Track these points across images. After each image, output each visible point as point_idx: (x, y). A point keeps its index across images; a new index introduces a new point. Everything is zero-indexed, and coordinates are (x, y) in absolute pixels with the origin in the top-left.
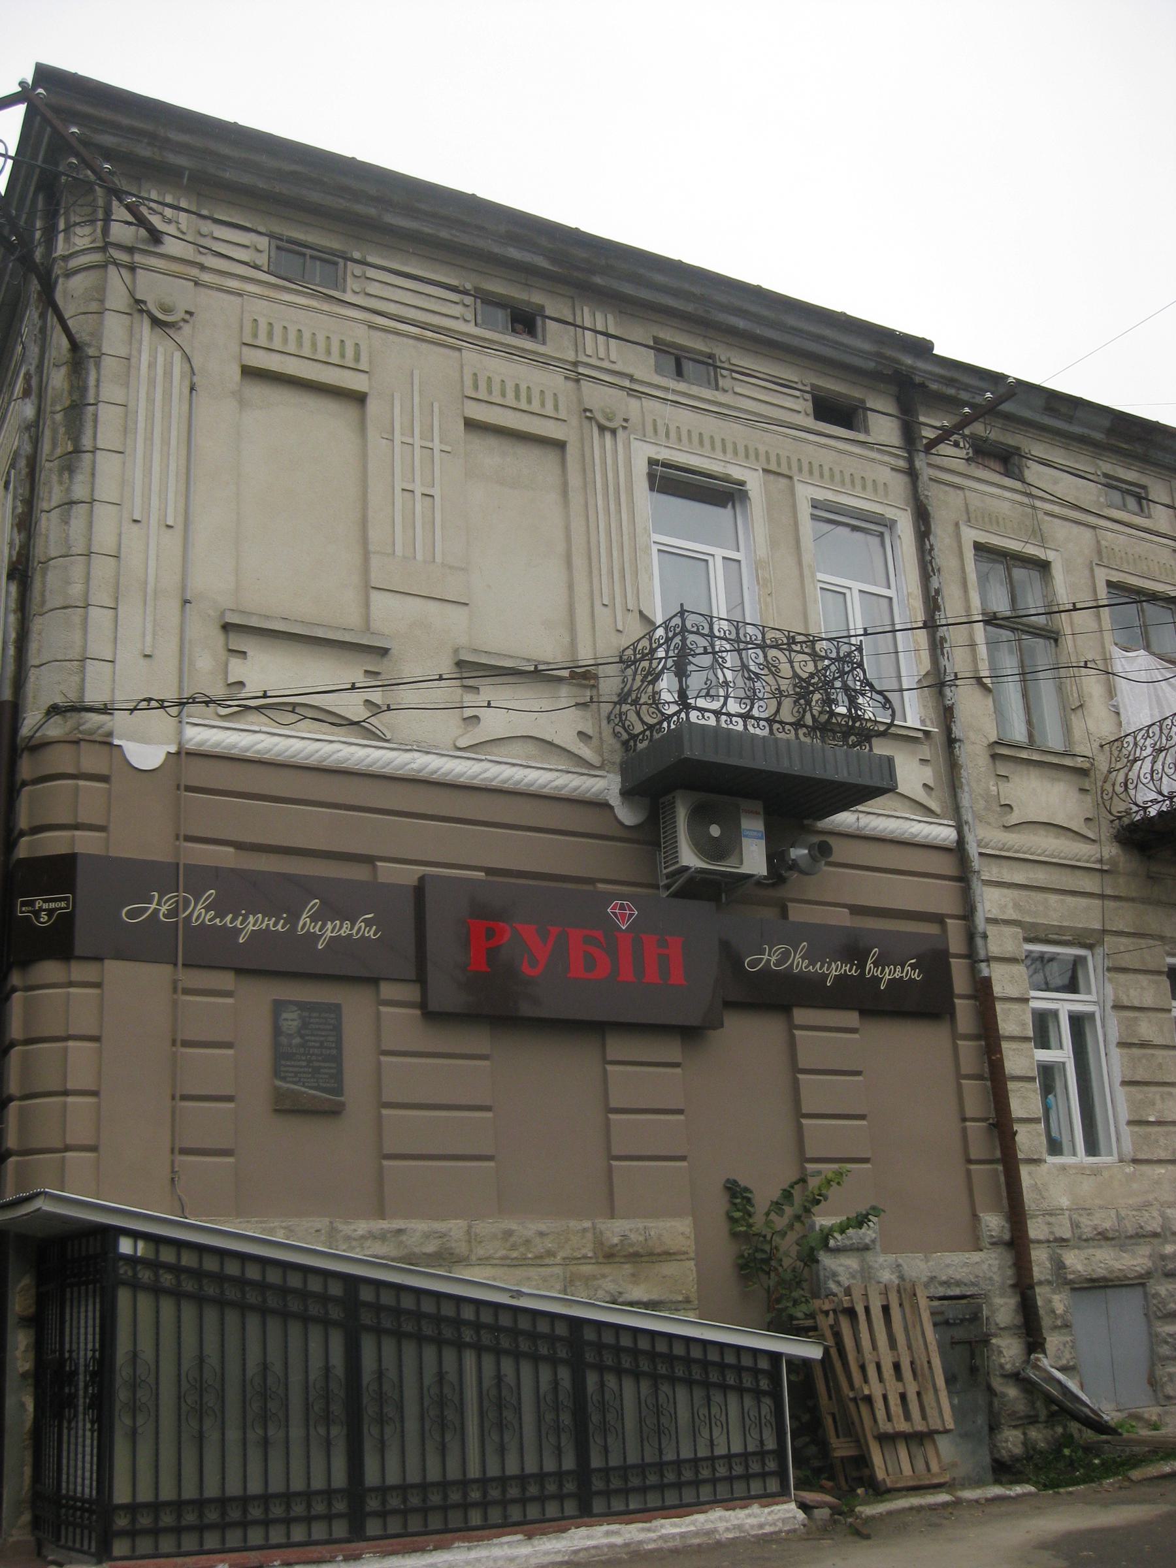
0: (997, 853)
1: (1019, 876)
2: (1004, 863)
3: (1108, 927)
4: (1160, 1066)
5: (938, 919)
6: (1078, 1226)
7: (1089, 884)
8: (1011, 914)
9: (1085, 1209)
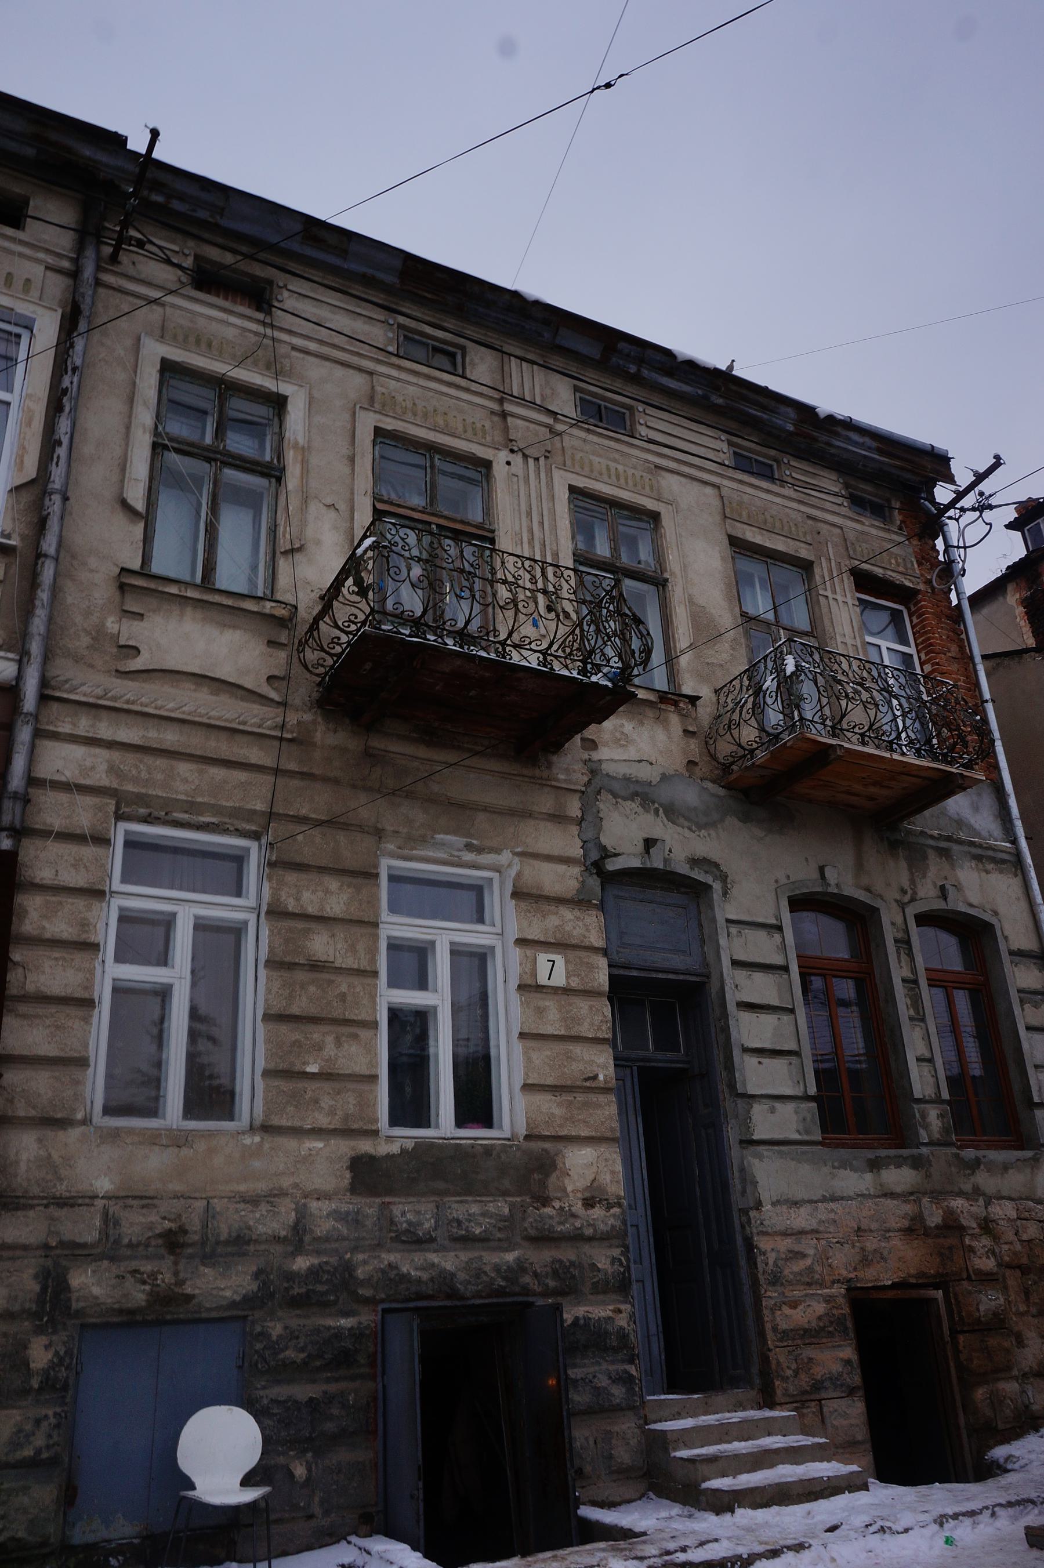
0: (91, 700)
1: (129, 733)
2: (104, 714)
3: (279, 809)
4: (343, 997)
6: (117, 1223)
7: (255, 754)
8: (101, 778)
9: (141, 1198)
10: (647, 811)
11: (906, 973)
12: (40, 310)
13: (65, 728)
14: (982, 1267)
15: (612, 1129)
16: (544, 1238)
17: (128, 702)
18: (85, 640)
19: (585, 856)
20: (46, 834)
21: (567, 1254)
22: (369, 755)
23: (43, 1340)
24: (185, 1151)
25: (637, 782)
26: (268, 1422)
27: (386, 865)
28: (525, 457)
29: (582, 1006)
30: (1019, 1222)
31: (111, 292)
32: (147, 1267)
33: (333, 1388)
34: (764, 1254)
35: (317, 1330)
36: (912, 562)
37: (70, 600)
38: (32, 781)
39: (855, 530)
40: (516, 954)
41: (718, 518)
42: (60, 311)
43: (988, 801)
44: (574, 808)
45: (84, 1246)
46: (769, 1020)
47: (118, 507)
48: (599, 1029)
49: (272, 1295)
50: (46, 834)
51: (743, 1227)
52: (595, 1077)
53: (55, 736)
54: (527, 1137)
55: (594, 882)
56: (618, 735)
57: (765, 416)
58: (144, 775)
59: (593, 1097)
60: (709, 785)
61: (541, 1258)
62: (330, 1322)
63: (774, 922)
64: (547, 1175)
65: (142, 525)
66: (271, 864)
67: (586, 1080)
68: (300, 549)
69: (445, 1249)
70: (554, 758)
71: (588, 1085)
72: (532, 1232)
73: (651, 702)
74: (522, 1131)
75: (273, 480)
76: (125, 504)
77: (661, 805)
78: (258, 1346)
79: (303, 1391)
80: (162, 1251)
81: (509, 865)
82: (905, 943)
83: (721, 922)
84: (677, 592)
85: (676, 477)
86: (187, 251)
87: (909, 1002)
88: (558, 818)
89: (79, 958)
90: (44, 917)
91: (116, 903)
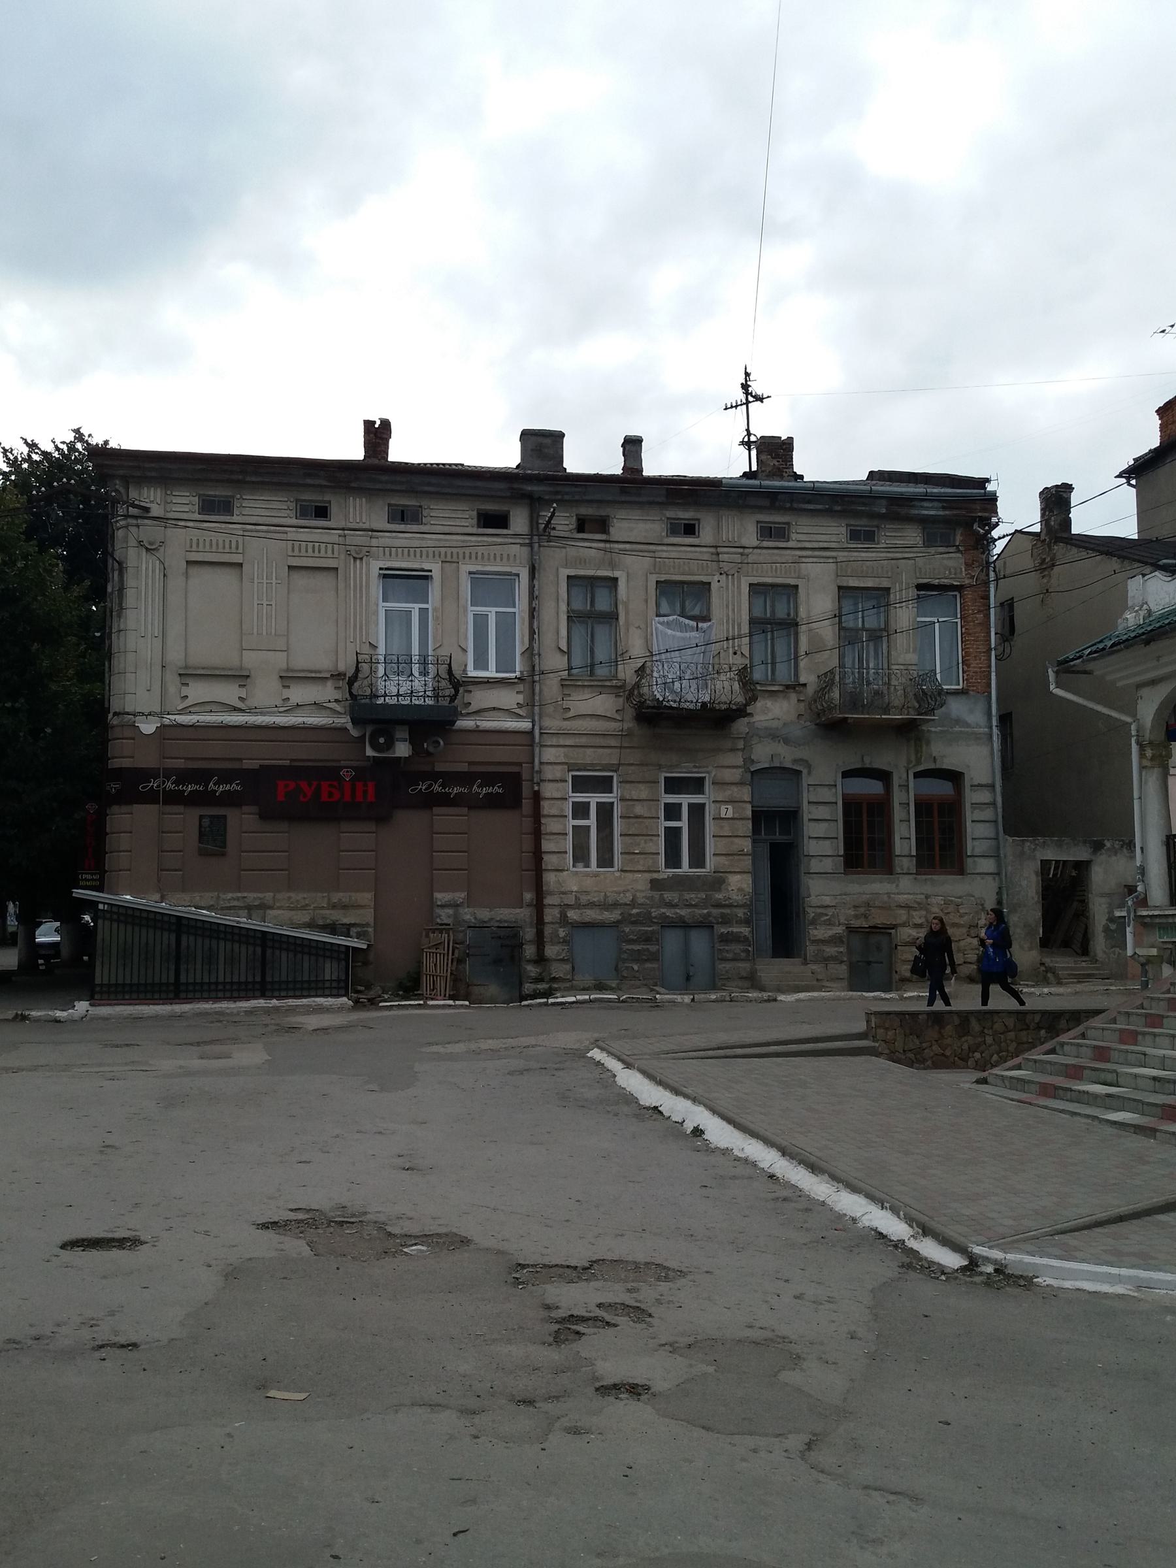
59: (741, 857)
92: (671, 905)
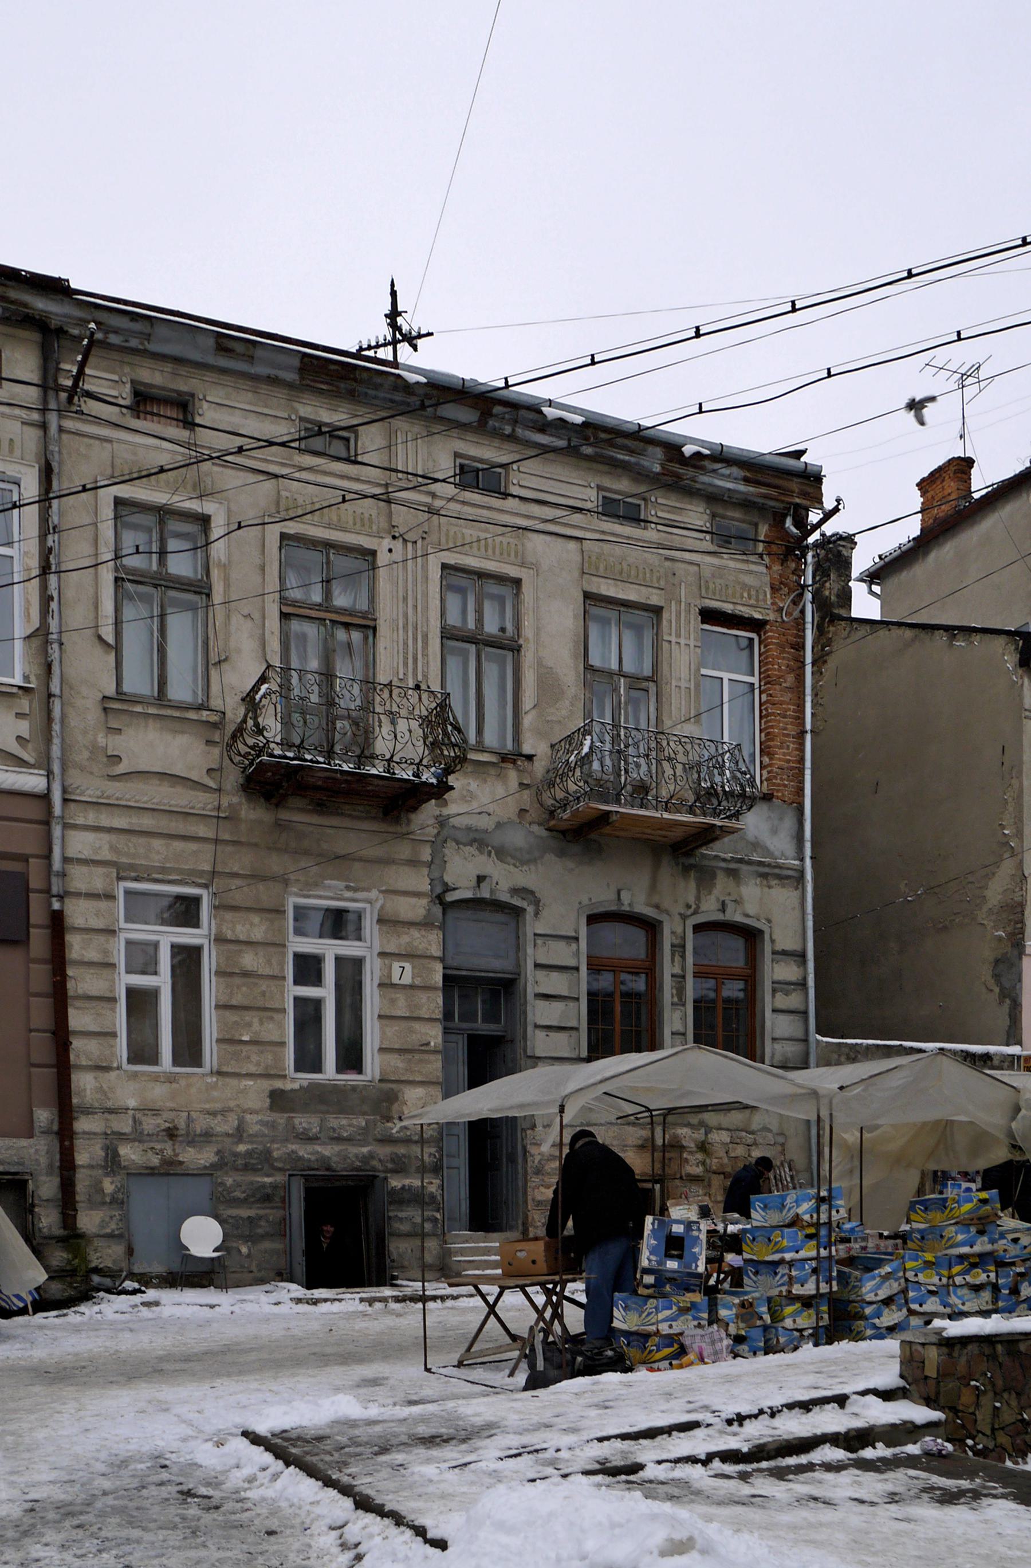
0: (94, 800)
1: (120, 821)
2: (103, 808)
3: (219, 869)
4: (263, 994)
5: (24, 859)
6: (141, 1123)
7: (202, 830)
8: (106, 855)
10: (482, 853)
11: (677, 970)
12: (23, 469)
13: (80, 821)
14: (692, 1172)
15: (438, 1077)
16: (387, 1140)
17: (117, 799)
18: (86, 754)
19: (432, 890)
20: (78, 895)
21: (402, 1150)
22: (279, 826)
23: (109, 1179)
24: (174, 1085)
25: (476, 830)
26: (226, 1226)
27: (292, 901)
28: (405, 541)
29: (423, 997)
30: (731, 1146)
31: (71, 436)
32: (158, 1146)
33: (261, 1212)
34: (532, 1156)
35: (252, 1183)
36: (765, 593)
37: (73, 724)
38: (66, 860)
39: (713, 565)
40: (378, 962)
41: (576, 574)
42: (37, 466)
43: (789, 823)
44: (426, 854)
45: (124, 1134)
46: (558, 1006)
47: (97, 641)
48: (433, 1012)
49: (226, 1164)
50: (78, 895)
51: (523, 1139)
52: (428, 1044)
53: (75, 827)
54: (380, 1081)
55: (438, 910)
56: (465, 793)
57: (633, 460)
58: (132, 850)
59: (426, 1057)
60: (535, 828)
61: (384, 1151)
62: (259, 1179)
63: (573, 934)
64: (392, 1104)
65: (113, 654)
66: (216, 907)
67: (422, 1045)
68: (226, 660)
69: (324, 1144)
70: (413, 816)
71: (424, 1048)
72: (379, 1137)
73: (494, 763)
74: (377, 1077)
75: (204, 596)
76: (100, 638)
77: (493, 847)
78: (220, 1189)
79: (245, 1213)
80: (166, 1138)
81: (377, 900)
82: (679, 948)
83: (530, 936)
84: (528, 657)
85: (542, 537)
86: (124, 379)
87: (675, 992)
88: (413, 863)
89: (106, 972)
90: (82, 948)
91: (123, 936)
92: (307, 1138)
